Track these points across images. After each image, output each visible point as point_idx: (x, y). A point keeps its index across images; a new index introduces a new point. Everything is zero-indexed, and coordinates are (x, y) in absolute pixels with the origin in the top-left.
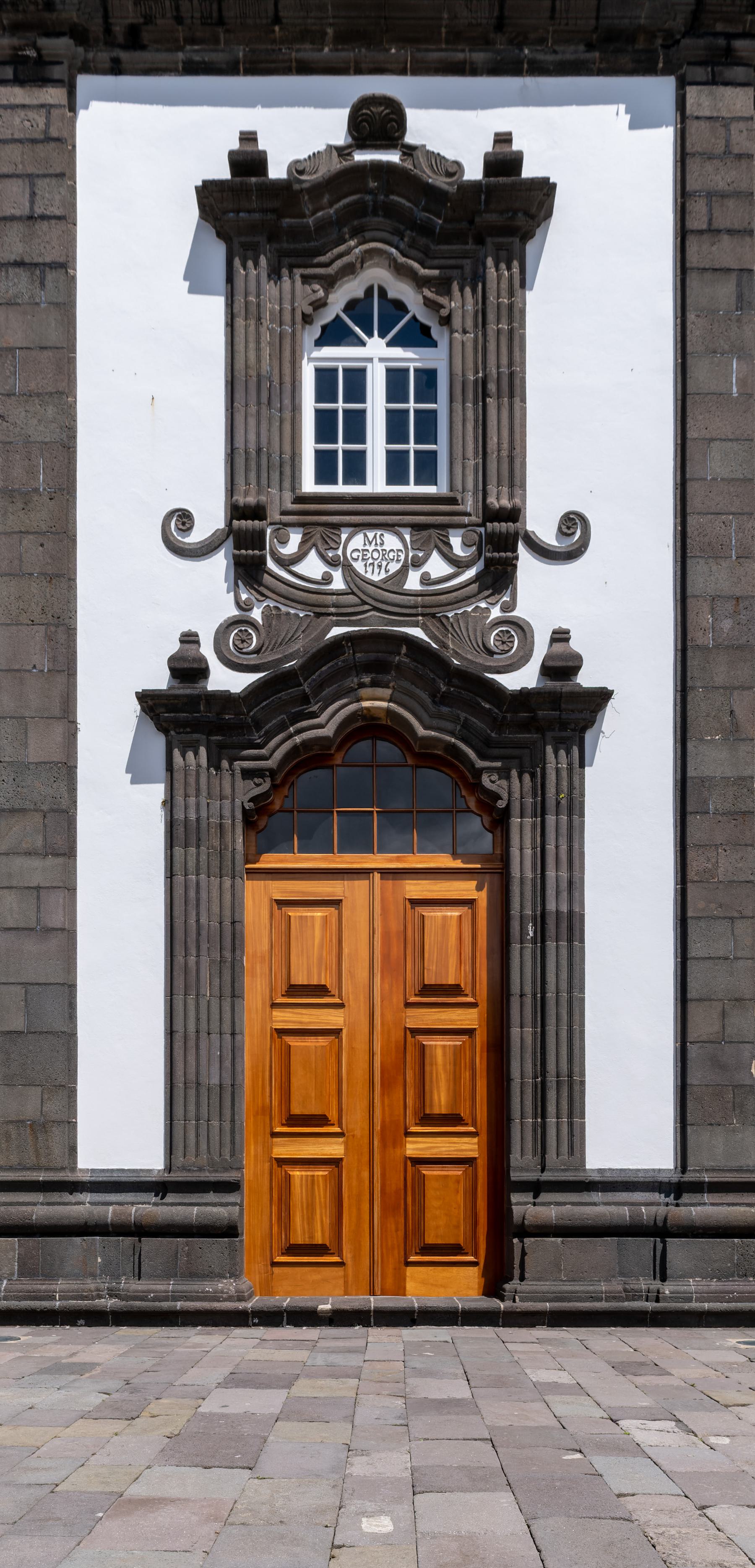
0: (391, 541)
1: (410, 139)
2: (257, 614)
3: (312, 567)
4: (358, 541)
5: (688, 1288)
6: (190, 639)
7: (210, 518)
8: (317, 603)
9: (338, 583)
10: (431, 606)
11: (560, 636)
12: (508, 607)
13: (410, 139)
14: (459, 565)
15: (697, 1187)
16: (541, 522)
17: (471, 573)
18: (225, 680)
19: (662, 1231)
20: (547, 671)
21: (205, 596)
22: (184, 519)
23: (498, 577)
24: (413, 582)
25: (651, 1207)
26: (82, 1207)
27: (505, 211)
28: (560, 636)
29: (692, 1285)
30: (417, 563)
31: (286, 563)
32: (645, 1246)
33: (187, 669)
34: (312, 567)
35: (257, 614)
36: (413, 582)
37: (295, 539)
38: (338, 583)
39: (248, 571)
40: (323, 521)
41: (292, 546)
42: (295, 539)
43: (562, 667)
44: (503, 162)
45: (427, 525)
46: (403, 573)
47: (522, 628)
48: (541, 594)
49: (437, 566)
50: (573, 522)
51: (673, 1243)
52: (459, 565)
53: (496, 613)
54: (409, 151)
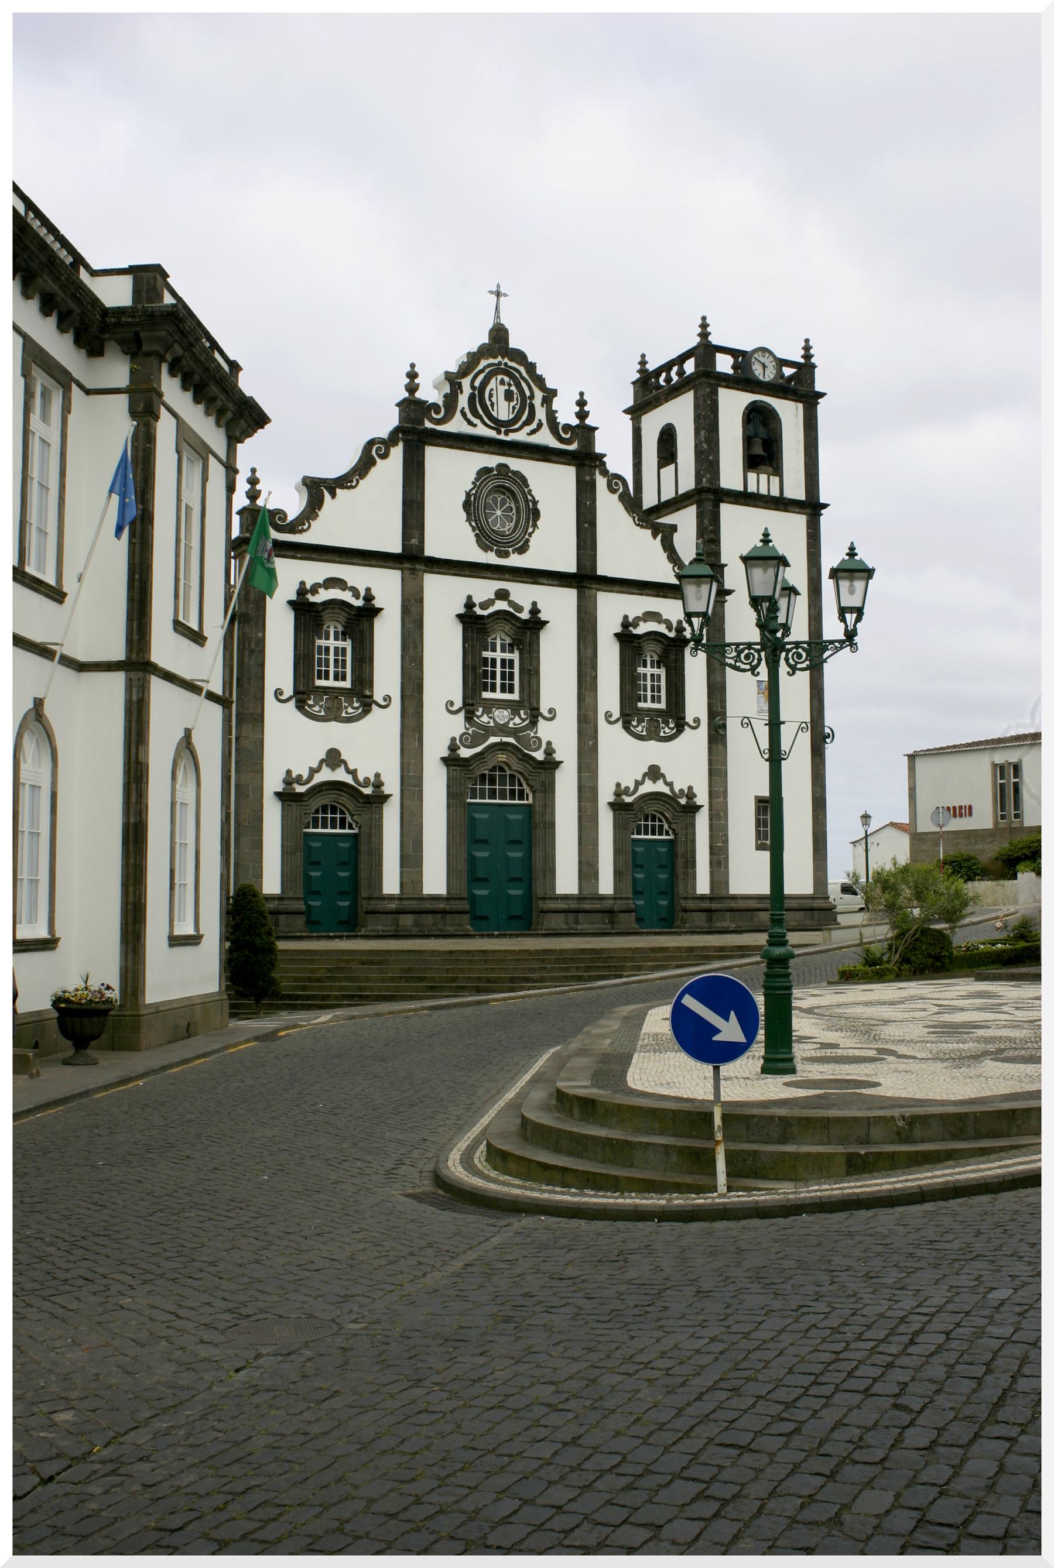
0: (506, 713)
1: (511, 598)
2: (470, 732)
3: (485, 719)
4: (497, 713)
5: (585, 927)
6: (453, 739)
7: (458, 703)
8: (488, 731)
9: (492, 724)
10: (515, 732)
11: (549, 743)
12: (536, 733)
13: (511, 598)
14: (523, 720)
15: (585, 899)
16: (544, 710)
17: (527, 722)
18: (465, 753)
19: (577, 912)
20: (545, 752)
21: (457, 725)
22: (452, 704)
23: (534, 723)
24: (511, 725)
25: (573, 905)
26: (427, 905)
27: (536, 624)
28: (549, 743)
29: (585, 926)
30: (512, 719)
31: (478, 717)
32: (571, 916)
33: (453, 748)
34: (485, 719)
35: (470, 732)
36: (511, 725)
37: (481, 709)
38: (492, 724)
39: (469, 718)
40: (490, 706)
41: (479, 713)
42: (481, 709)
43: (550, 751)
44: (535, 611)
45: (514, 707)
46: (508, 722)
47: (539, 739)
48: (545, 730)
49: (517, 720)
50: (551, 711)
51: (580, 915)
52: (523, 720)
53: (532, 734)
54: (511, 604)
